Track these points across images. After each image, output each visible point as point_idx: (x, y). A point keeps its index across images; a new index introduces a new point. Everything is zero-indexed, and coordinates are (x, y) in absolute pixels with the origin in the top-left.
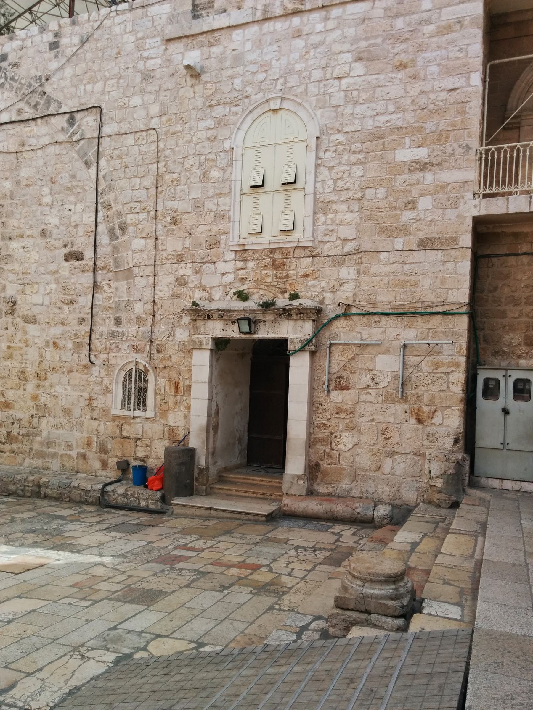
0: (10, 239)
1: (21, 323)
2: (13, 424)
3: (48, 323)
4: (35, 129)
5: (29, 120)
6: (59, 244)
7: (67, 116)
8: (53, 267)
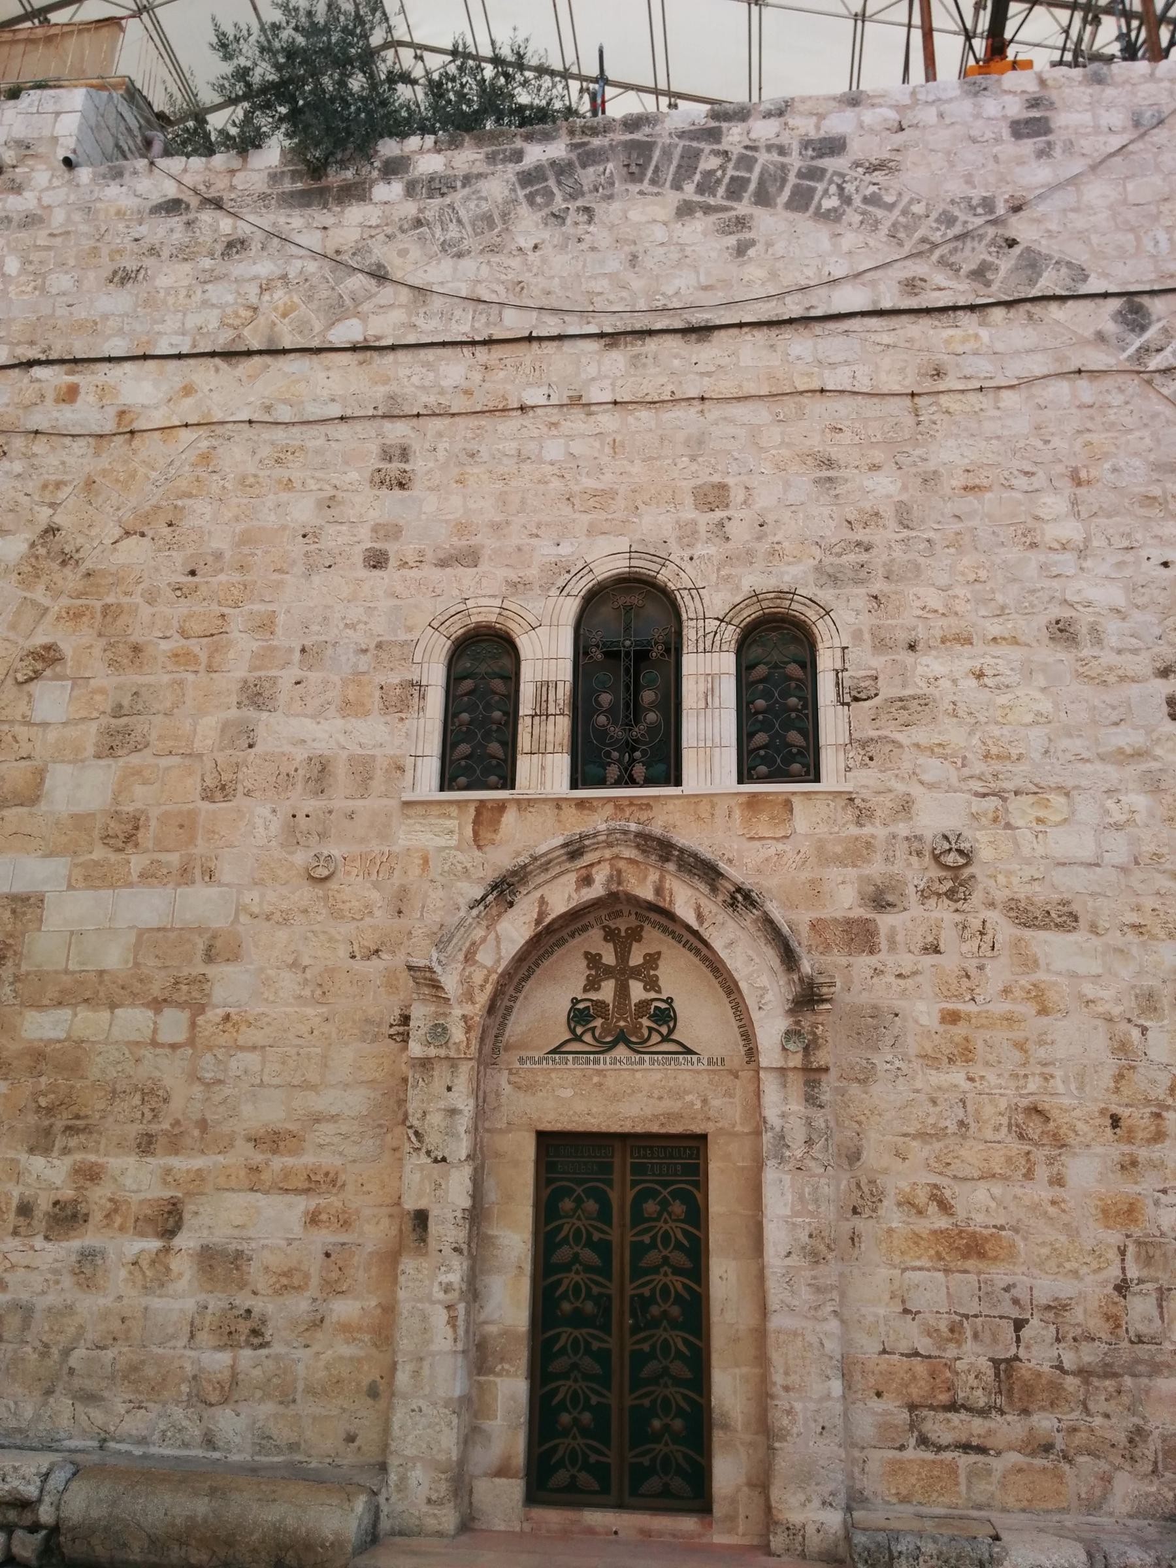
0: (912, 647)
1: (1004, 930)
2: (1019, 1325)
3: (1134, 926)
4: (984, 333)
5: (955, 308)
6: (1142, 664)
7: (1115, 304)
8: (1126, 738)
